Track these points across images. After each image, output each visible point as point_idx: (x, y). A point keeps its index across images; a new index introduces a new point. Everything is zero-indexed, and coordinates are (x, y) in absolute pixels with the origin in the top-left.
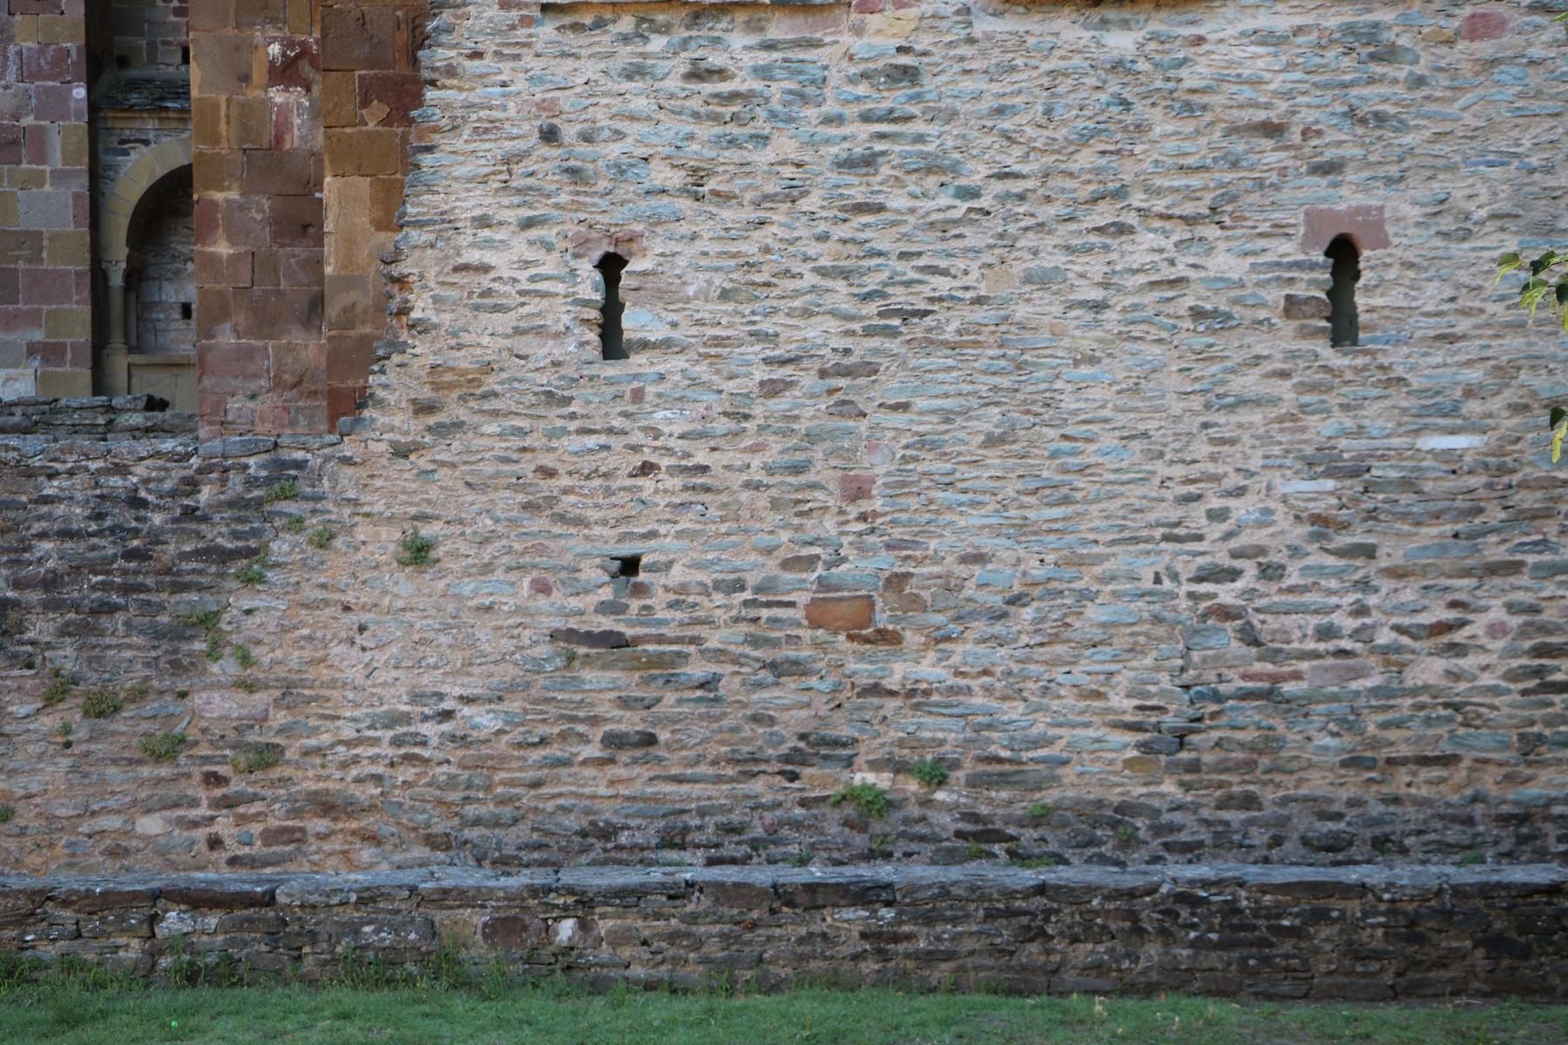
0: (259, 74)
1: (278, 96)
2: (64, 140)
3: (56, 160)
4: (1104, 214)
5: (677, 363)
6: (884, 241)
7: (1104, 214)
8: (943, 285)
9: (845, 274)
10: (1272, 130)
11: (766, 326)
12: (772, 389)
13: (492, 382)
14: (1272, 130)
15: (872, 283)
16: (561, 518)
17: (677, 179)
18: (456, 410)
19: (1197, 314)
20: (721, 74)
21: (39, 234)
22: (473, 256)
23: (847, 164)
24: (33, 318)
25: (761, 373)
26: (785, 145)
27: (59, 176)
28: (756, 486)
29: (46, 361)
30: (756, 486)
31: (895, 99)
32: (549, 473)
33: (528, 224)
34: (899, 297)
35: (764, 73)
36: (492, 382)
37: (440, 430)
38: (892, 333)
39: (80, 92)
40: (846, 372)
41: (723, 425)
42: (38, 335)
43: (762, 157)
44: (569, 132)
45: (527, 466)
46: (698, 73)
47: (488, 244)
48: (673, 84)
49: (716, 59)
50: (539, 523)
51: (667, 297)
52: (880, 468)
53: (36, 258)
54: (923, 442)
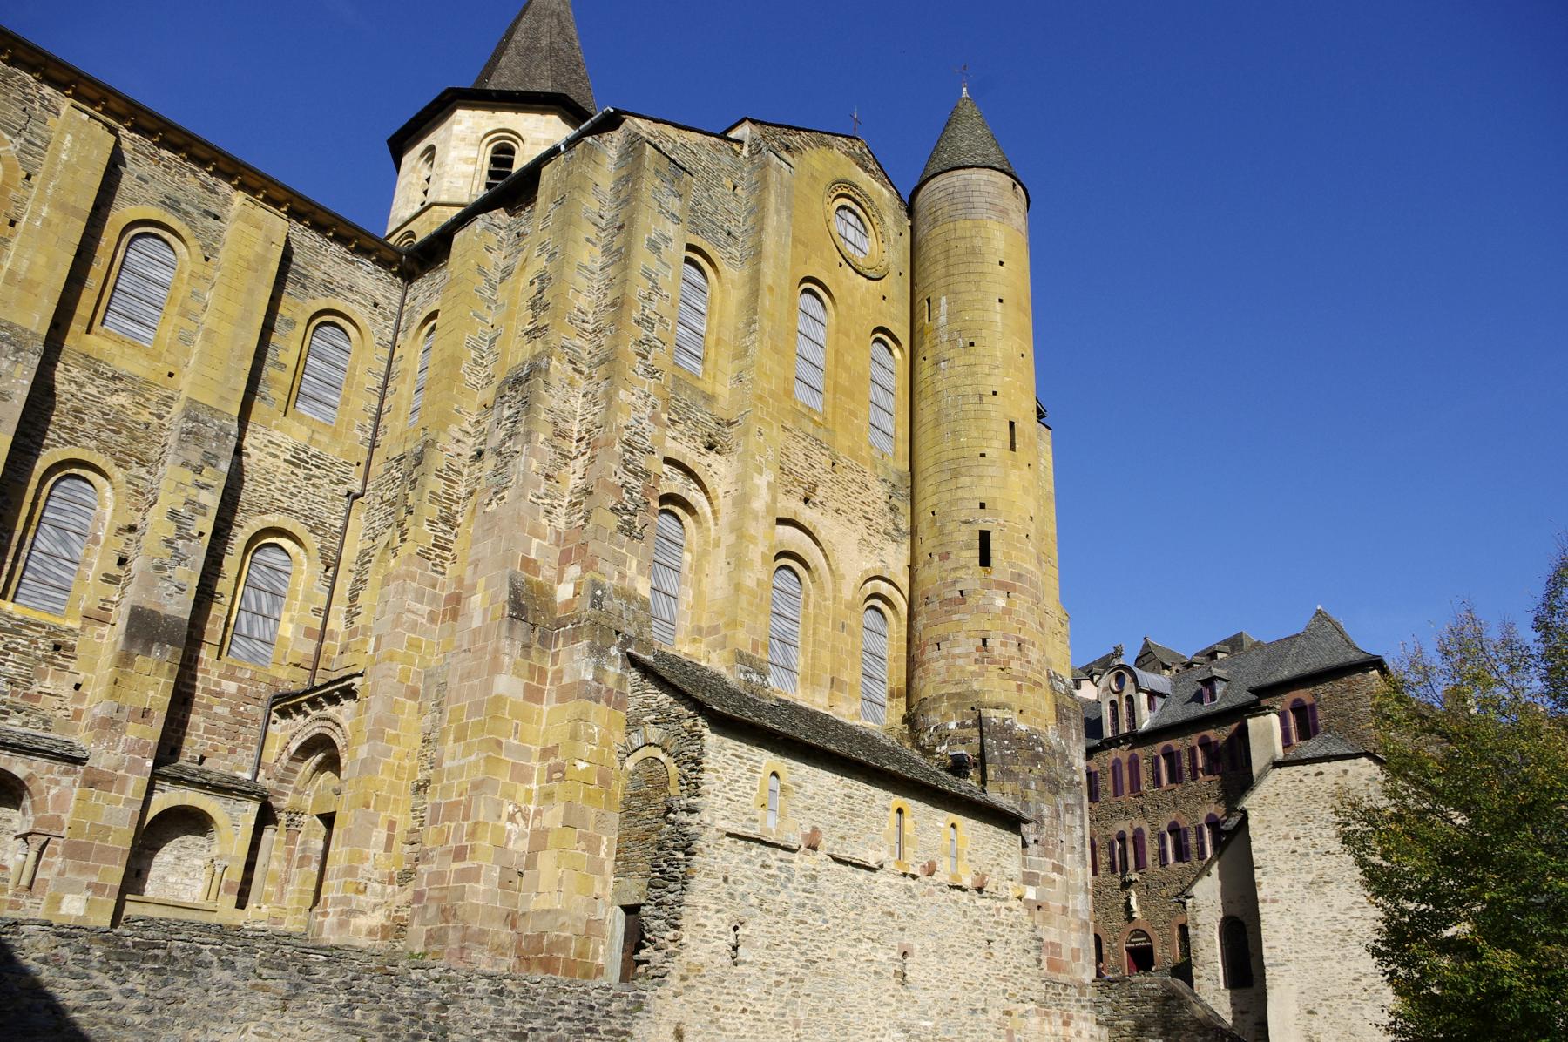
0: (504, 817)
1: (509, 826)
2: (136, 784)
3: (129, 794)
4: (855, 935)
5: (753, 971)
6: (806, 934)
7: (855, 935)
8: (820, 953)
9: (797, 944)
10: (891, 914)
11: (777, 960)
12: (778, 984)
13: (704, 971)
14: (891, 914)
15: (803, 948)
16: (719, 1028)
17: (756, 902)
18: (692, 981)
19: (876, 973)
20: (769, 867)
21: (109, 829)
22: (702, 921)
23: (799, 906)
24: (95, 870)
25: (775, 978)
26: (783, 896)
27: (128, 802)
28: (771, 1020)
29: (95, 893)
30: (771, 1020)
31: (809, 885)
32: (717, 1009)
33: (718, 911)
34: (811, 956)
35: (779, 868)
36: (704, 971)
37: (688, 988)
38: (807, 968)
39: (150, 764)
40: (796, 980)
41: (764, 996)
42: (95, 879)
43: (778, 898)
44: (731, 879)
45: (711, 1006)
46: (764, 866)
47: (706, 917)
48: (757, 868)
49: (768, 862)
50: (713, 1029)
51: (752, 945)
52: (802, 1016)
53: (105, 840)
54: (814, 1009)
